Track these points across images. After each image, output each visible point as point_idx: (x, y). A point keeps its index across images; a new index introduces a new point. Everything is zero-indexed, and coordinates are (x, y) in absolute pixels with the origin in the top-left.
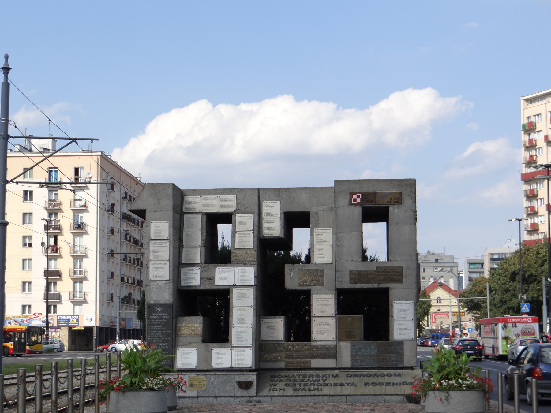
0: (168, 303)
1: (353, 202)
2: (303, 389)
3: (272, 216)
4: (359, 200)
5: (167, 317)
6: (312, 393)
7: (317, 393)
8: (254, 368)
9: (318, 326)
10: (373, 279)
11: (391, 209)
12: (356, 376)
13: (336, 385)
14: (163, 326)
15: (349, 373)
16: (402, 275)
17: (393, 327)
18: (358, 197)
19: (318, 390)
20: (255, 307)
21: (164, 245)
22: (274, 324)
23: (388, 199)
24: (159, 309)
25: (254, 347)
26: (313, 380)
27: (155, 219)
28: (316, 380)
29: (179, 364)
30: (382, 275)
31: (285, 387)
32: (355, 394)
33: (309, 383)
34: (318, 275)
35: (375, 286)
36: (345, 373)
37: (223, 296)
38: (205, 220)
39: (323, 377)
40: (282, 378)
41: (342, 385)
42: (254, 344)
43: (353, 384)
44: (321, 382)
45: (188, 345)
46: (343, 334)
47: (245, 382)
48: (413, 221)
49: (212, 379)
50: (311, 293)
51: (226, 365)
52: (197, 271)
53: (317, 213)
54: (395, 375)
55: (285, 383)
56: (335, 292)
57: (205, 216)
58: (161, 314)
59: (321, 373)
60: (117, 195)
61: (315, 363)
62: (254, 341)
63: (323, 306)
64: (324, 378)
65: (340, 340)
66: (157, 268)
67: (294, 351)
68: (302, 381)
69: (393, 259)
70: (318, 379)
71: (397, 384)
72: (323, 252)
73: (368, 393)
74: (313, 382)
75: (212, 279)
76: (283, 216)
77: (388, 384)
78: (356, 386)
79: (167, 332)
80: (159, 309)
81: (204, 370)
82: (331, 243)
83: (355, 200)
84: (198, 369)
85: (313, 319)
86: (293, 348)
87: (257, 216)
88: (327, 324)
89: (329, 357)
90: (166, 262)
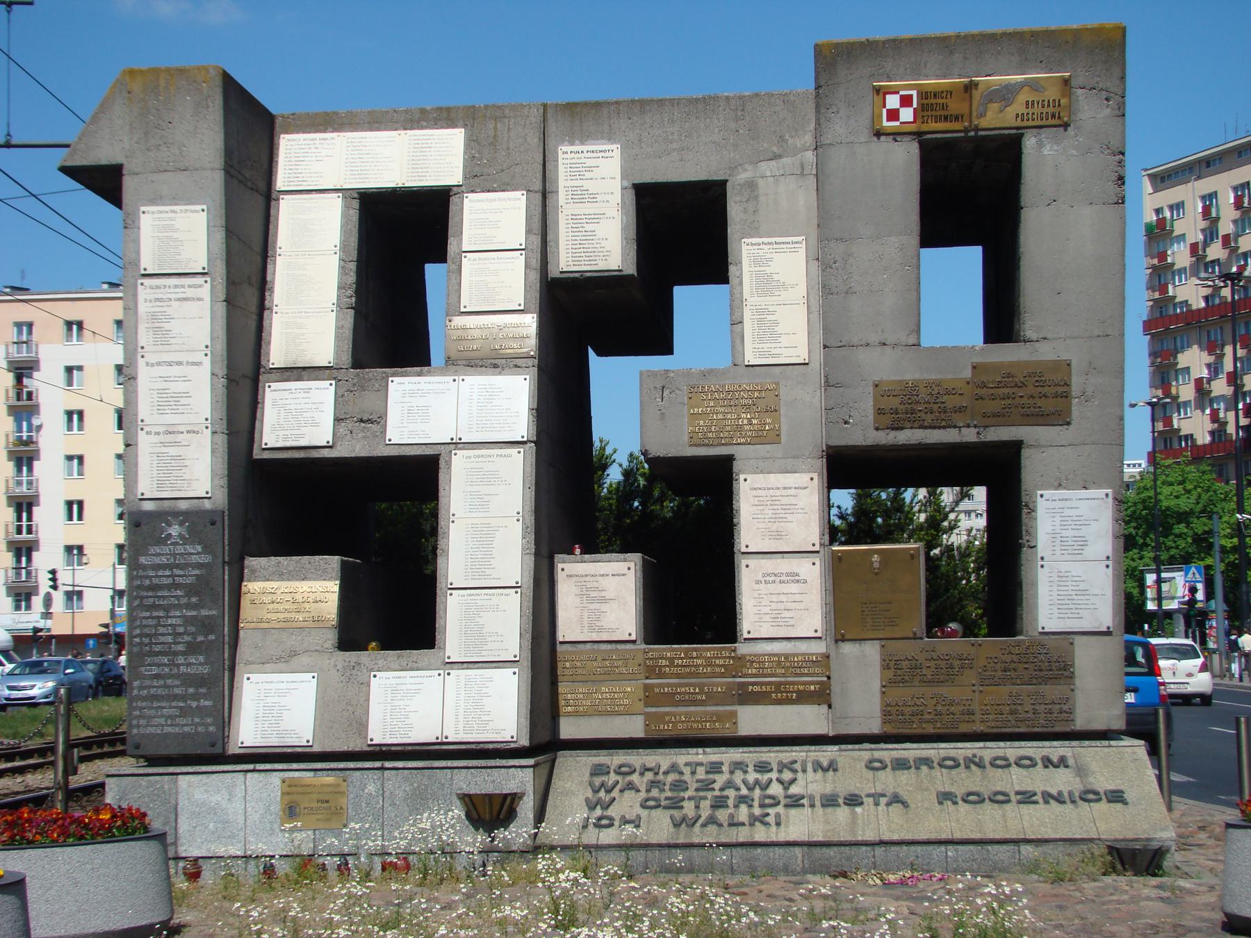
0: (207, 505)
1: (885, 124)
2: (712, 820)
3: (593, 198)
4: (907, 114)
5: (205, 559)
6: (742, 835)
7: (760, 834)
8: (525, 742)
9: (762, 586)
10: (960, 410)
11: (1029, 143)
12: (901, 765)
13: (830, 801)
14: (190, 590)
15: (877, 754)
16: (1066, 396)
17: (1034, 585)
18: (906, 101)
19: (766, 824)
20: (531, 520)
21: (190, 293)
22: (604, 583)
23: (1018, 107)
24: (175, 530)
25: (527, 663)
26: (744, 782)
27: (156, 200)
28: (757, 782)
29: (249, 732)
30: (993, 398)
31: (644, 813)
32: (909, 837)
33: (731, 793)
36: (863, 753)
37: (413, 482)
38: (355, 215)
39: (780, 771)
40: (635, 778)
41: (853, 801)
42: (527, 654)
43: (896, 799)
44: (776, 789)
45: (284, 660)
46: (849, 611)
47: (490, 797)
48: (1111, 188)
49: (371, 788)
50: (737, 466)
51: (421, 728)
52: (323, 394)
53: (751, 185)
54: (1047, 762)
55: (643, 795)
56: (821, 464)
57: (356, 204)
58: (180, 549)
59: (772, 755)
61: (753, 719)
62: (527, 644)
64: (787, 775)
65: (840, 639)
66: (166, 379)
67: (678, 676)
68: (706, 786)
69: (1034, 336)
70: (765, 777)
71: (1059, 799)
72: (776, 323)
73: (958, 835)
74: (744, 791)
75: (377, 420)
76: (631, 195)
77: (1027, 798)
78: (905, 804)
79: (204, 612)
80: (175, 530)
82: (802, 290)
83: (893, 115)
84: (316, 749)
85: (744, 562)
86: (672, 665)
87: (539, 197)
88: (794, 578)
89: (803, 698)
90: (199, 357)
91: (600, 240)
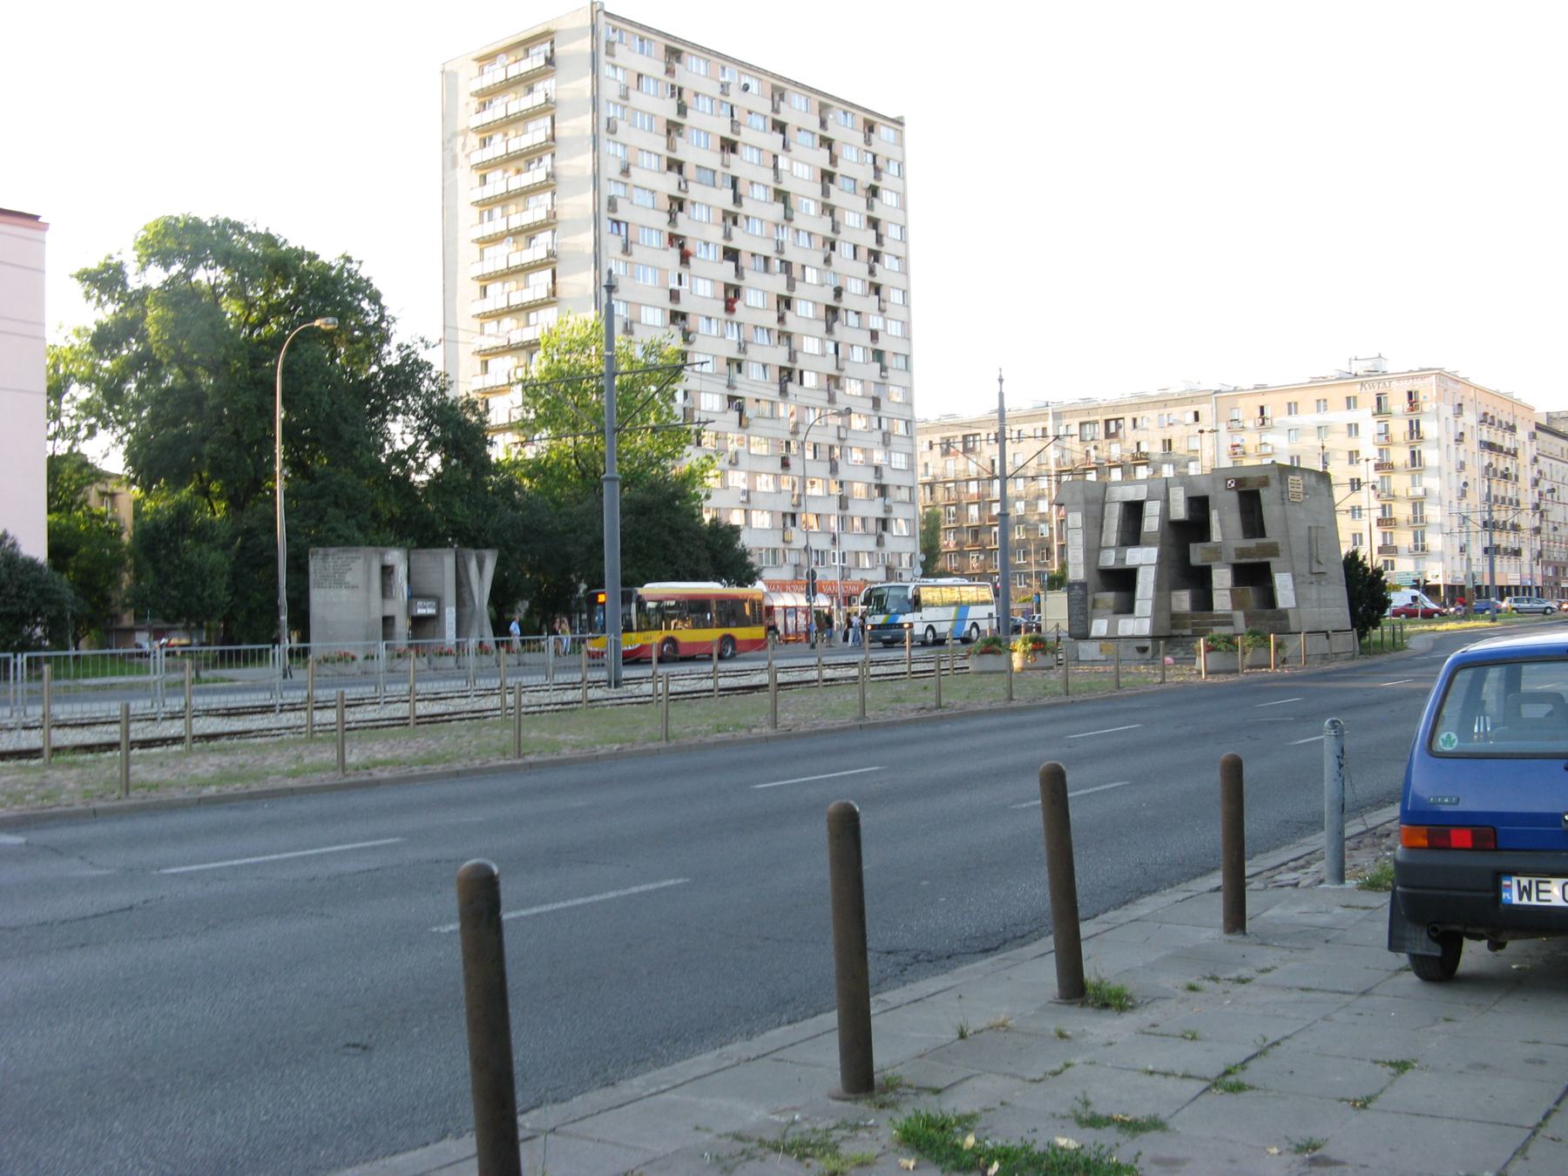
29: (1093, 634)
34: (1217, 552)
35: (1257, 560)
46: (1237, 603)
52: (1113, 553)
60: (1470, 418)
63: (1222, 579)
81: (1112, 638)
91: (1179, 511)
